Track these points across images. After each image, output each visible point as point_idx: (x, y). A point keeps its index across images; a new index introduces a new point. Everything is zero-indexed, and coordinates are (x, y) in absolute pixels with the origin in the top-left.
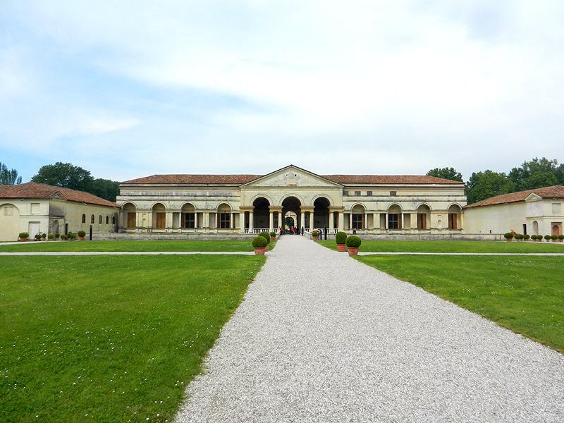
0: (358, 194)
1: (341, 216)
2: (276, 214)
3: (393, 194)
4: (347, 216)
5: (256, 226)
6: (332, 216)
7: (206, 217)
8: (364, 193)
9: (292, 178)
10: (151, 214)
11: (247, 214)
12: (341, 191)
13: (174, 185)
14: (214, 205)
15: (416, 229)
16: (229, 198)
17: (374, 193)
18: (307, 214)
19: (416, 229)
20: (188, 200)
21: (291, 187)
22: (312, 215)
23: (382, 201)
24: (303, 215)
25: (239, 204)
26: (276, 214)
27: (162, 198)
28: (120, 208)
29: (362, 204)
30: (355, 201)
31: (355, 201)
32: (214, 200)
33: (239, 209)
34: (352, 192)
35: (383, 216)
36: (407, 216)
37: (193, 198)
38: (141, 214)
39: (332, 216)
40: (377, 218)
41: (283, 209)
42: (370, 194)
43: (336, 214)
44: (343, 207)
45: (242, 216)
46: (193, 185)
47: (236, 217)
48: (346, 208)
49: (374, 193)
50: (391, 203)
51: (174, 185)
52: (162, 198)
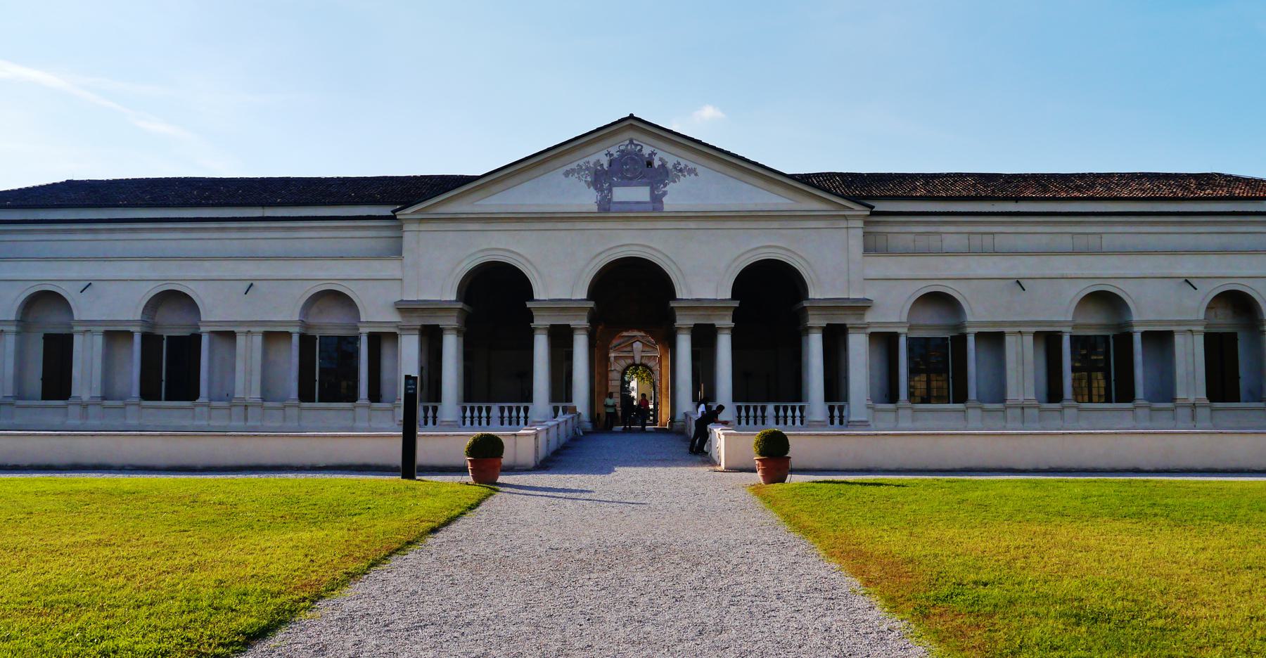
2: (561, 339)
5: (472, 392)
6: (815, 346)
7: (249, 350)
11: (431, 339)
21: (629, 213)
22: (724, 345)
24: (684, 344)
26: (561, 339)
33: (395, 317)
35: (1049, 341)
36: (1161, 340)
39: (815, 346)
41: (594, 318)
43: (835, 339)
44: (861, 307)
47: (386, 350)
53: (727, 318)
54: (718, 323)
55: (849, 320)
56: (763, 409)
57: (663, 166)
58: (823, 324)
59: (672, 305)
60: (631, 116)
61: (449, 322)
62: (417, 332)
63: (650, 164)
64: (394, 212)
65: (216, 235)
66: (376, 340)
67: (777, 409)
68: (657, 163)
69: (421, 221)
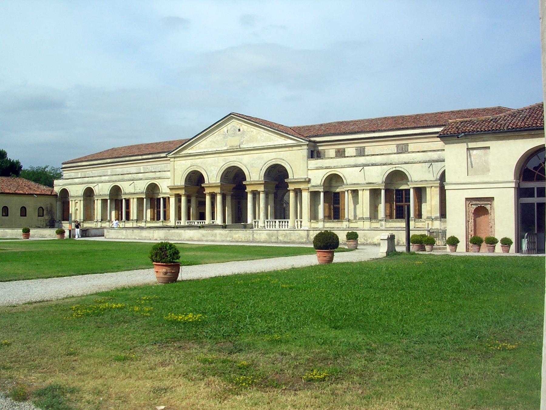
0: (340, 154)
1: (306, 196)
3: (402, 150)
4: (314, 195)
8: (350, 150)
9: (234, 135)
10: (82, 202)
11: (178, 197)
12: (304, 152)
13: (109, 161)
14: (142, 186)
15: (436, 219)
16: (158, 174)
17: (368, 151)
18: (213, 196)
19: (436, 219)
20: (116, 181)
23: (373, 165)
25: (169, 183)
26: (213, 196)
27: (90, 179)
28: (56, 195)
29: (339, 172)
30: (327, 168)
31: (327, 168)
32: (141, 179)
33: (168, 191)
34: (331, 151)
35: (375, 193)
37: (121, 177)
38: (74, 202)
40: (365, 197)
42: (361, 153)
45: (172, 200)
46: (127, 159)
48: (313, 183)
49: (370, 148)
50: (389, 169)
51: (109, 161)
52: (90, 179)
53: (262, 187)
54: (259, 190)
55: (302, 186)
56: (275, 222)
57: (244, 131)
58: (293, 188)
59: (244, 183)
60: (230, 114)
61: (182, 192)
62: (174, 196)
63: (239, 130)
64: (166, 155)
65: (132, 165)
66: (164, 199)
67: (280, 222)
68: (241, 130)
69: (174, 158)
